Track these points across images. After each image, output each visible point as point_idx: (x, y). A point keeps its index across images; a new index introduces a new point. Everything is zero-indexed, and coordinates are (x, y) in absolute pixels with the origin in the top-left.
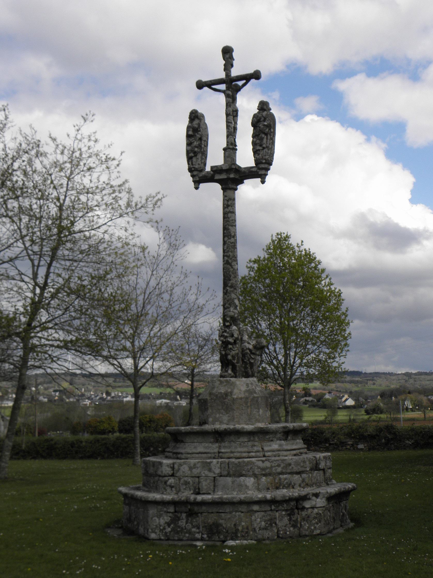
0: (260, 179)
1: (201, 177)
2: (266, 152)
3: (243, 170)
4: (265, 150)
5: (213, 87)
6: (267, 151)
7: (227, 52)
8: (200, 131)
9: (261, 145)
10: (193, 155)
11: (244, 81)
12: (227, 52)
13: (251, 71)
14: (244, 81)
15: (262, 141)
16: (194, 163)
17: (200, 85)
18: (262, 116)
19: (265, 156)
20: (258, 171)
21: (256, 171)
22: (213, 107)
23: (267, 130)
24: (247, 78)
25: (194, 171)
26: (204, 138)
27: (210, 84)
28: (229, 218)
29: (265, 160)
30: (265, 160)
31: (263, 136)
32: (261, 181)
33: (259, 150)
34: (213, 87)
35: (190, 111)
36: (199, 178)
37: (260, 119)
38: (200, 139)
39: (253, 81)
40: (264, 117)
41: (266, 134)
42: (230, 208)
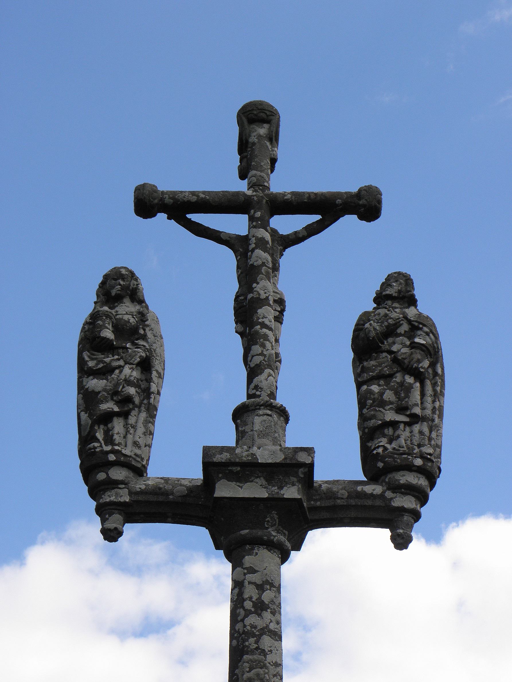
0: (386, 533)
1: (142, 492)
2: (421, 433)
3: (324, 487)
4: (416, 428)
5: (194, 217)
6: (426, 430)
7: (257, 121)
8: (144, 337)
9: (401, 409)
10: (116, 409)
11: (317, 217)
12: (257, 121)
13: (350, 185)
14: (317, 217)
15: (407, 396)
16: (117, 438)
17: (148, 203)
18: (406, 318)
19: (419, 446)
20: (389, 494)
21: (382, 496)
22: (189, 286)
23: (426, 363)
24: (328, 209)
25: (113, 464)
26: (156, 364)
27: (180, 208)
28: (264, 653)
29: (422, 456)
30: (422, 456)
31: (410, 380)
32: (393, 539)
33: (394, 424)
34: (194, 217)
35: (106, 270)
36: (130, 493)
37: (397, 325)
38: (146, 365)
39: (349, 222)
40: (409, 322)
41: (419, 376)
42: (267, 615)
